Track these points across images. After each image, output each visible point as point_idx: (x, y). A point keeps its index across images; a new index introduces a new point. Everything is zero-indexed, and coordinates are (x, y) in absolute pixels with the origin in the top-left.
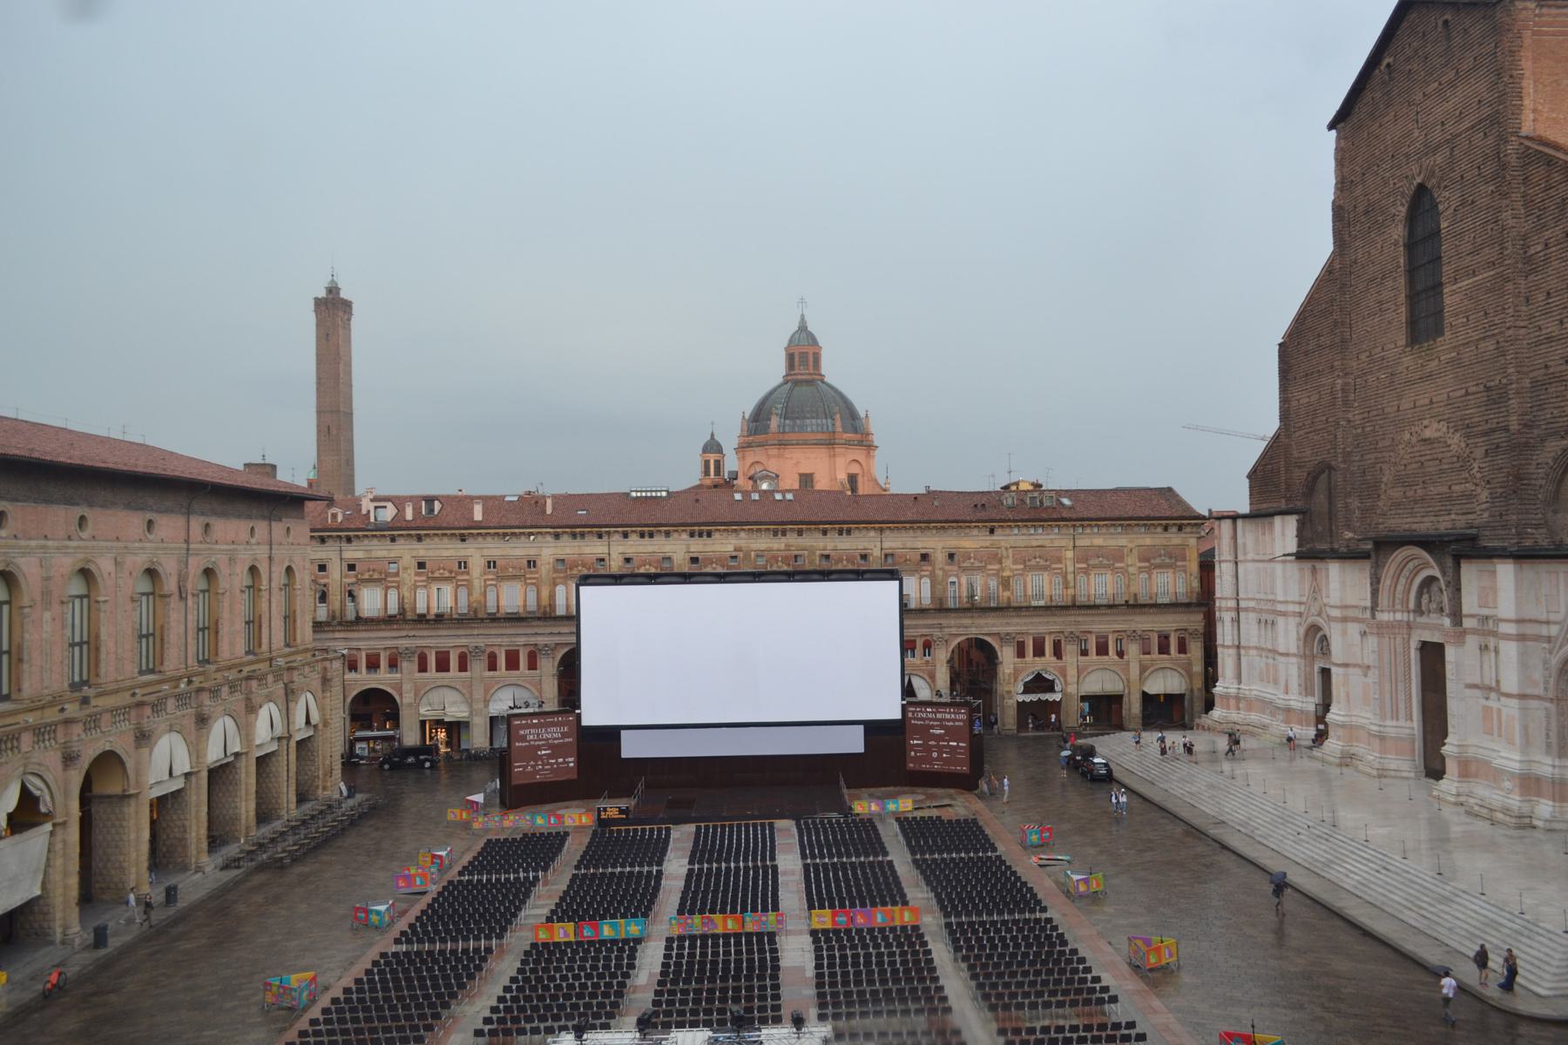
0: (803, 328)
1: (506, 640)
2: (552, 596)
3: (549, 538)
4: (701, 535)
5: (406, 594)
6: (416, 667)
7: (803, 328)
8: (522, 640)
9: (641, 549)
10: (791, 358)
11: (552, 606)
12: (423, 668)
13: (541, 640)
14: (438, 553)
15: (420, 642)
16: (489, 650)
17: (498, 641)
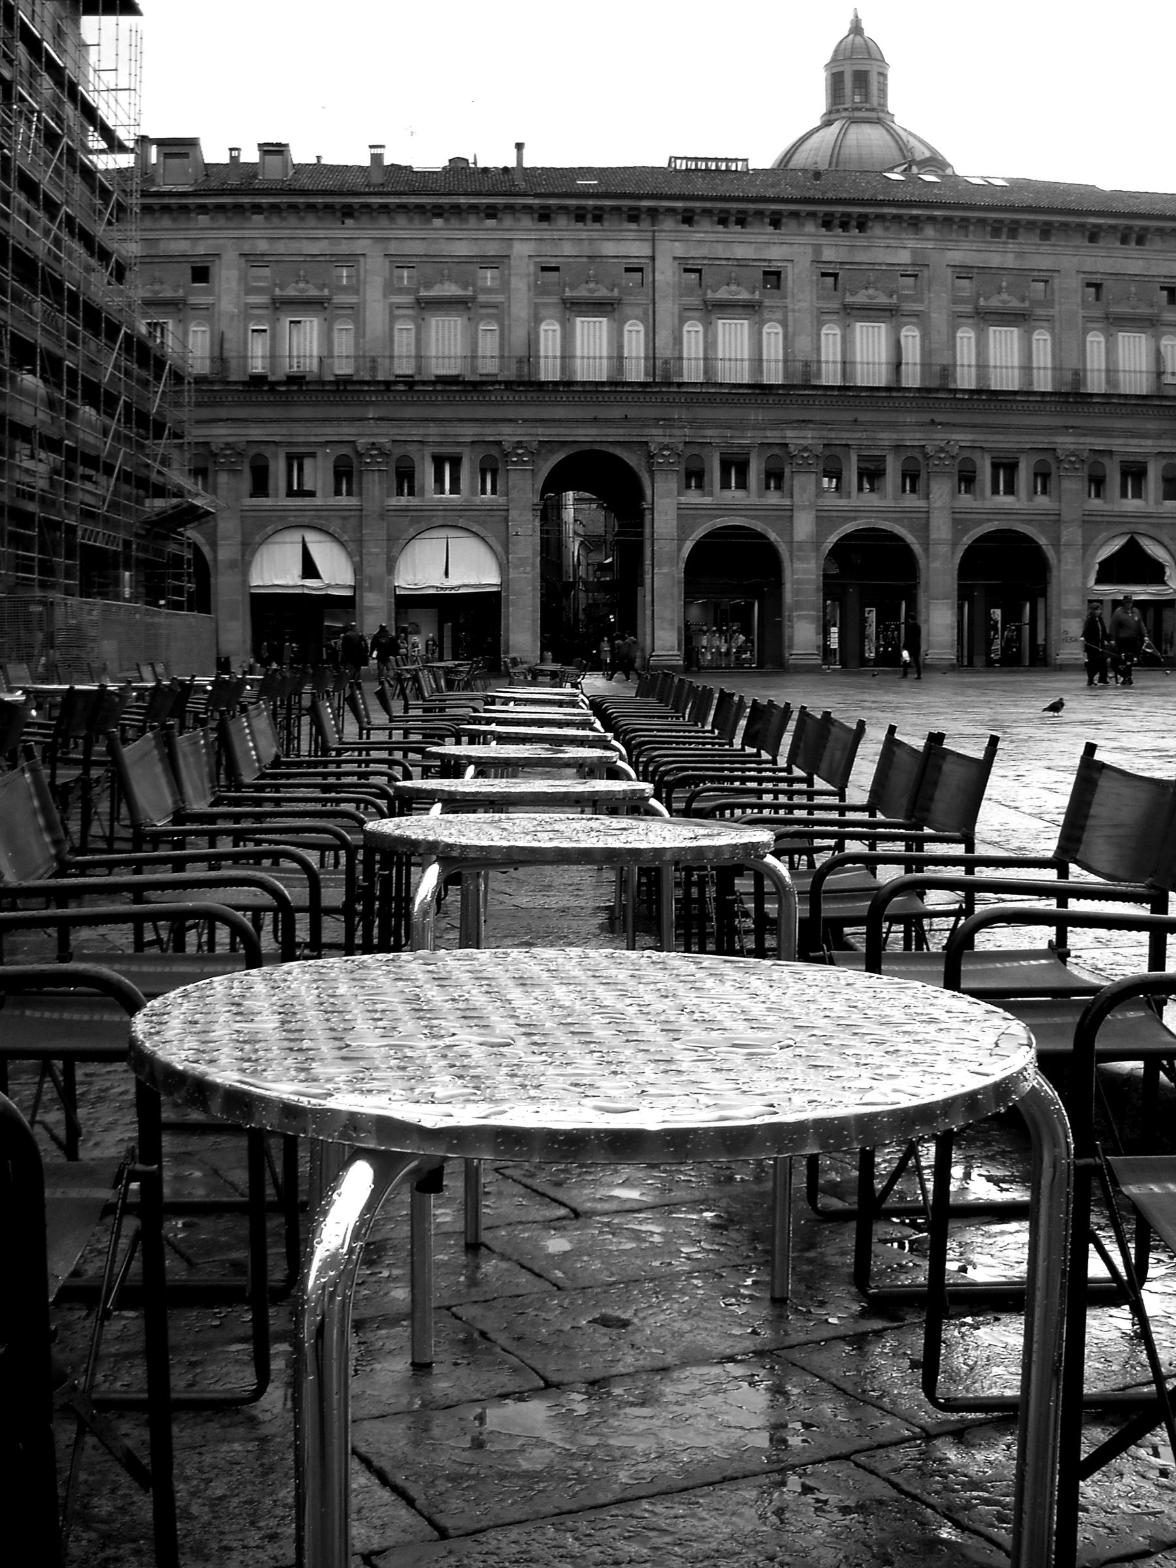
0: (856, 28)
1: (433, 431)
2: (532, 342)
3: (527, 222)
4: (844, 226)
5: (230, 335)
6: (246, 483)
7: (856, 28)
8: (468, 432)
9: (721, 251)
10: (836, 82)
11: (530, 357)
12: (260, 487)
13: (508, 434)
14: (294, 247)
15: (256, 433)
16: (398, 451)
17: (416, 432)
